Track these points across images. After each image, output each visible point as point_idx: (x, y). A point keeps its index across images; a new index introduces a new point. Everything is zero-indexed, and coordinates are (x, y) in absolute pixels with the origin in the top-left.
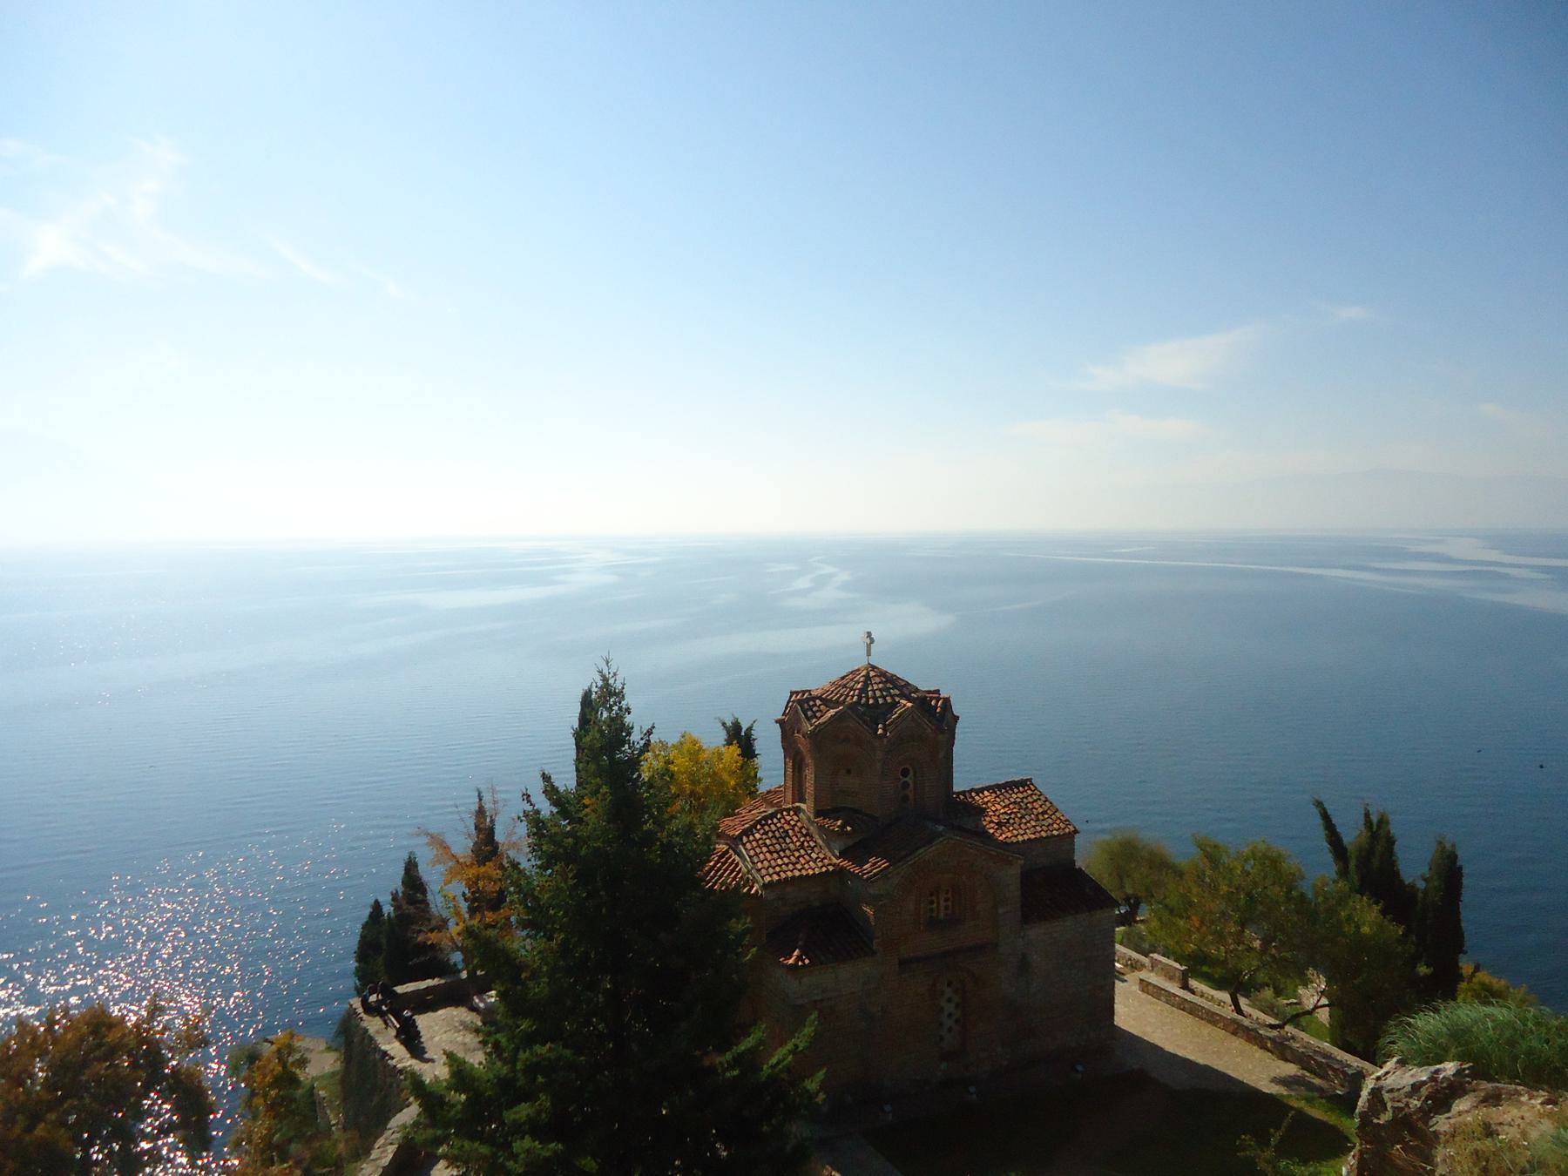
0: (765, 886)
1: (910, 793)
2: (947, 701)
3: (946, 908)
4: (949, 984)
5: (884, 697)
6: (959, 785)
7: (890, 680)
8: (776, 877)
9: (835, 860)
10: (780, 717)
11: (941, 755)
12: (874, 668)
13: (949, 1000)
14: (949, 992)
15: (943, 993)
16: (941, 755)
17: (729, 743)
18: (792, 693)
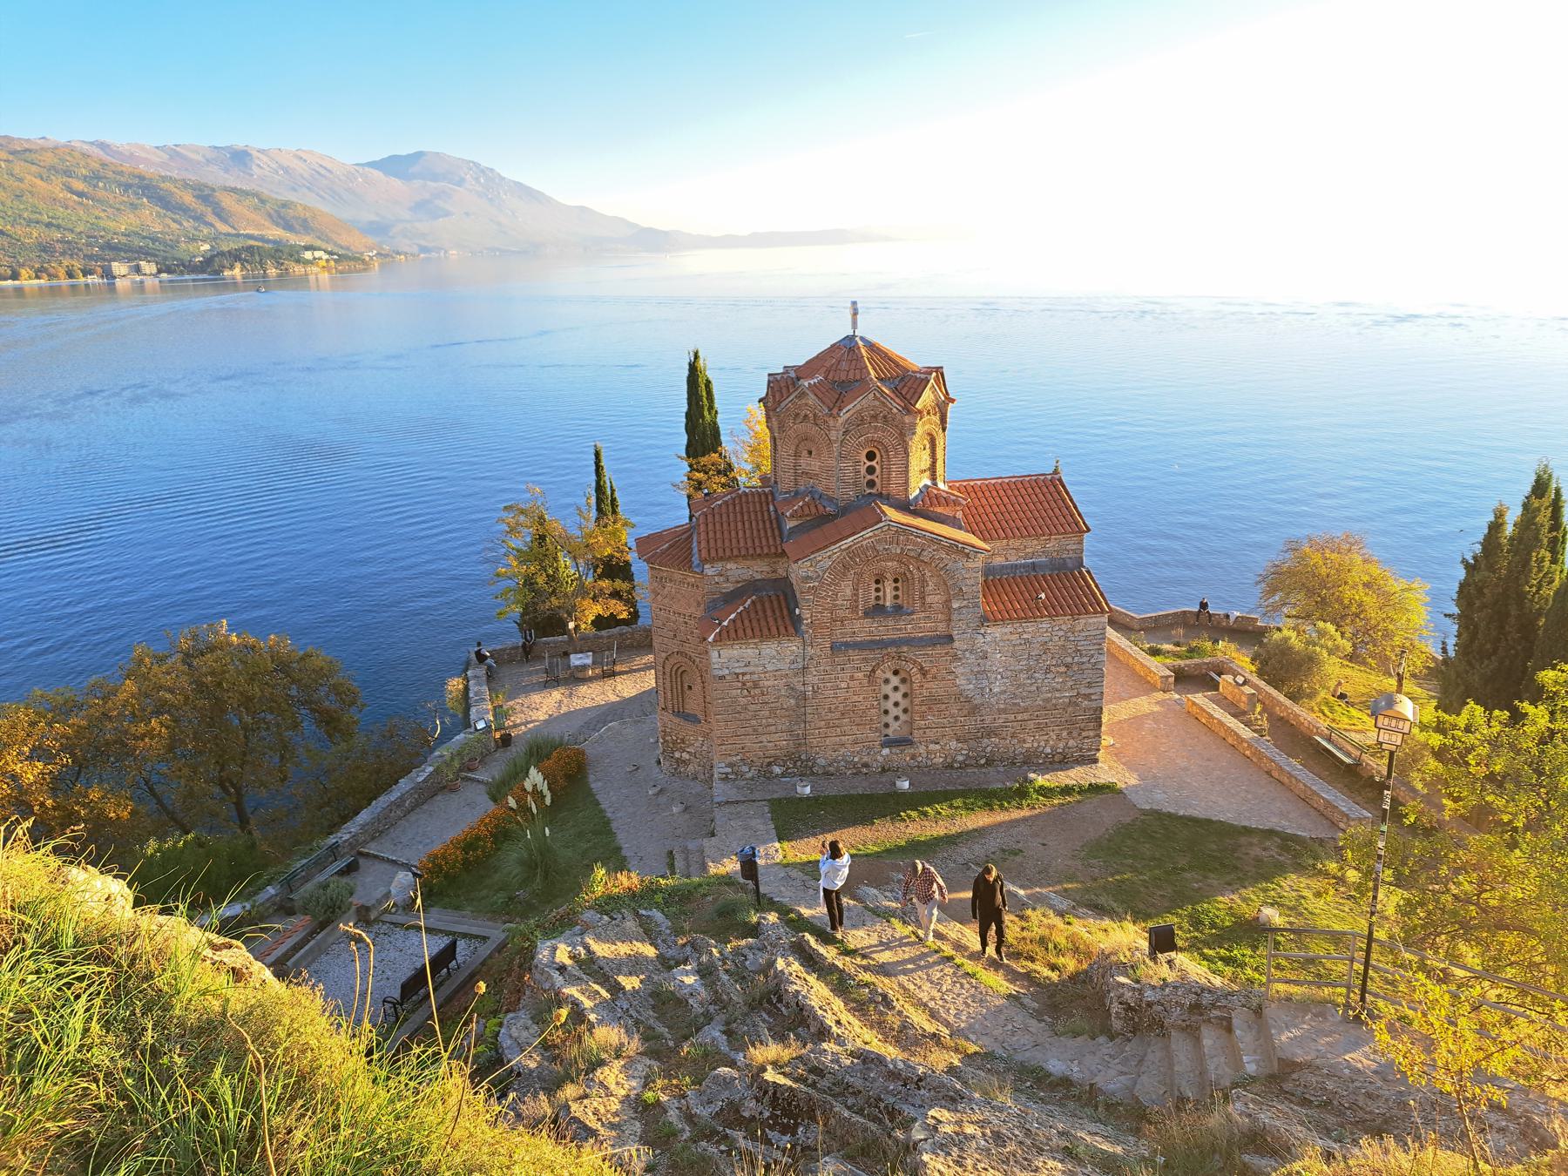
3: (896, 597)
4: (896, 673)
13: (896, 689)
14: (895, 681)
15: (887, 681)
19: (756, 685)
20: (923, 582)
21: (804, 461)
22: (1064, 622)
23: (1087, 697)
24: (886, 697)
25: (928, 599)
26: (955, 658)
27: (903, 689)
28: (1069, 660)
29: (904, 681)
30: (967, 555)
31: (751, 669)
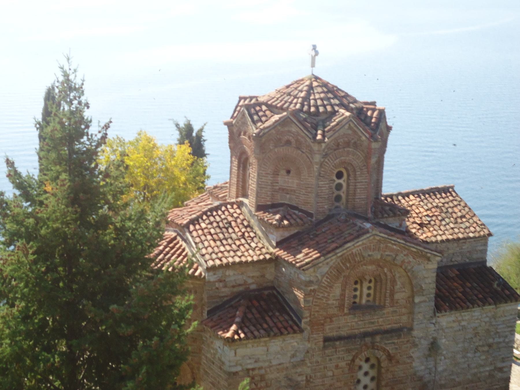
0: (208, 269)
1: (343, 193)
2: (382, 113)
3: (369, 295)
4: (367, 360)
5: (324, 106)
6: (387, 189)
7: (332, 91)
8: (218, 262)
9: (272, 250)
10: (228, 119)
11: (373, 160)
12: (317, 78)
13: (366, 374)
14: (366, 367)
15: (360, 368)
16: (373, 160)
17: (181, 142)
18: (241, 98)
19: (262, 378)
20: (394, 282)
21: (283, 180)
22: (489, 309)
23: (500, 370)
24: (359, 381)
25: (397, 296)
26: (415, 345)
27: (373, 373)
28: (491, 341)
29: (372, 366)
30: (429, 259)
31: (260, 364)
